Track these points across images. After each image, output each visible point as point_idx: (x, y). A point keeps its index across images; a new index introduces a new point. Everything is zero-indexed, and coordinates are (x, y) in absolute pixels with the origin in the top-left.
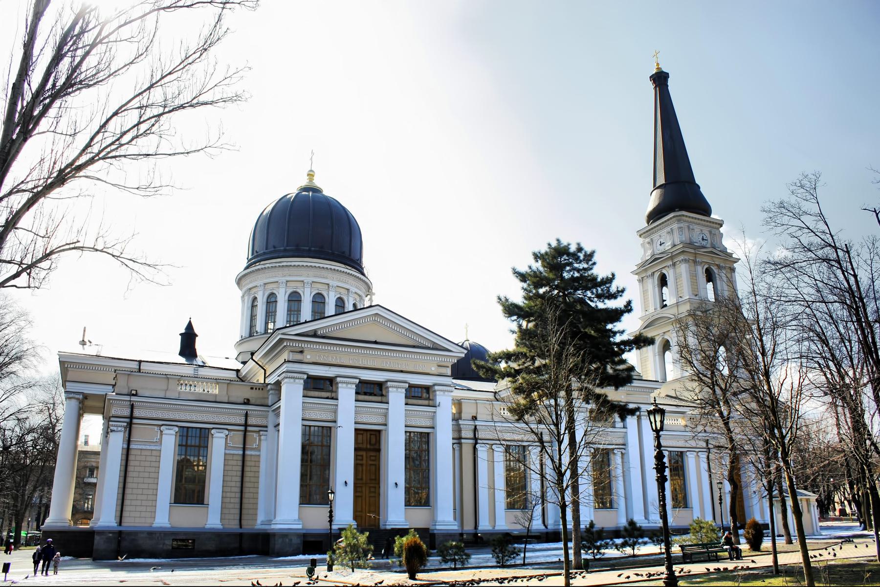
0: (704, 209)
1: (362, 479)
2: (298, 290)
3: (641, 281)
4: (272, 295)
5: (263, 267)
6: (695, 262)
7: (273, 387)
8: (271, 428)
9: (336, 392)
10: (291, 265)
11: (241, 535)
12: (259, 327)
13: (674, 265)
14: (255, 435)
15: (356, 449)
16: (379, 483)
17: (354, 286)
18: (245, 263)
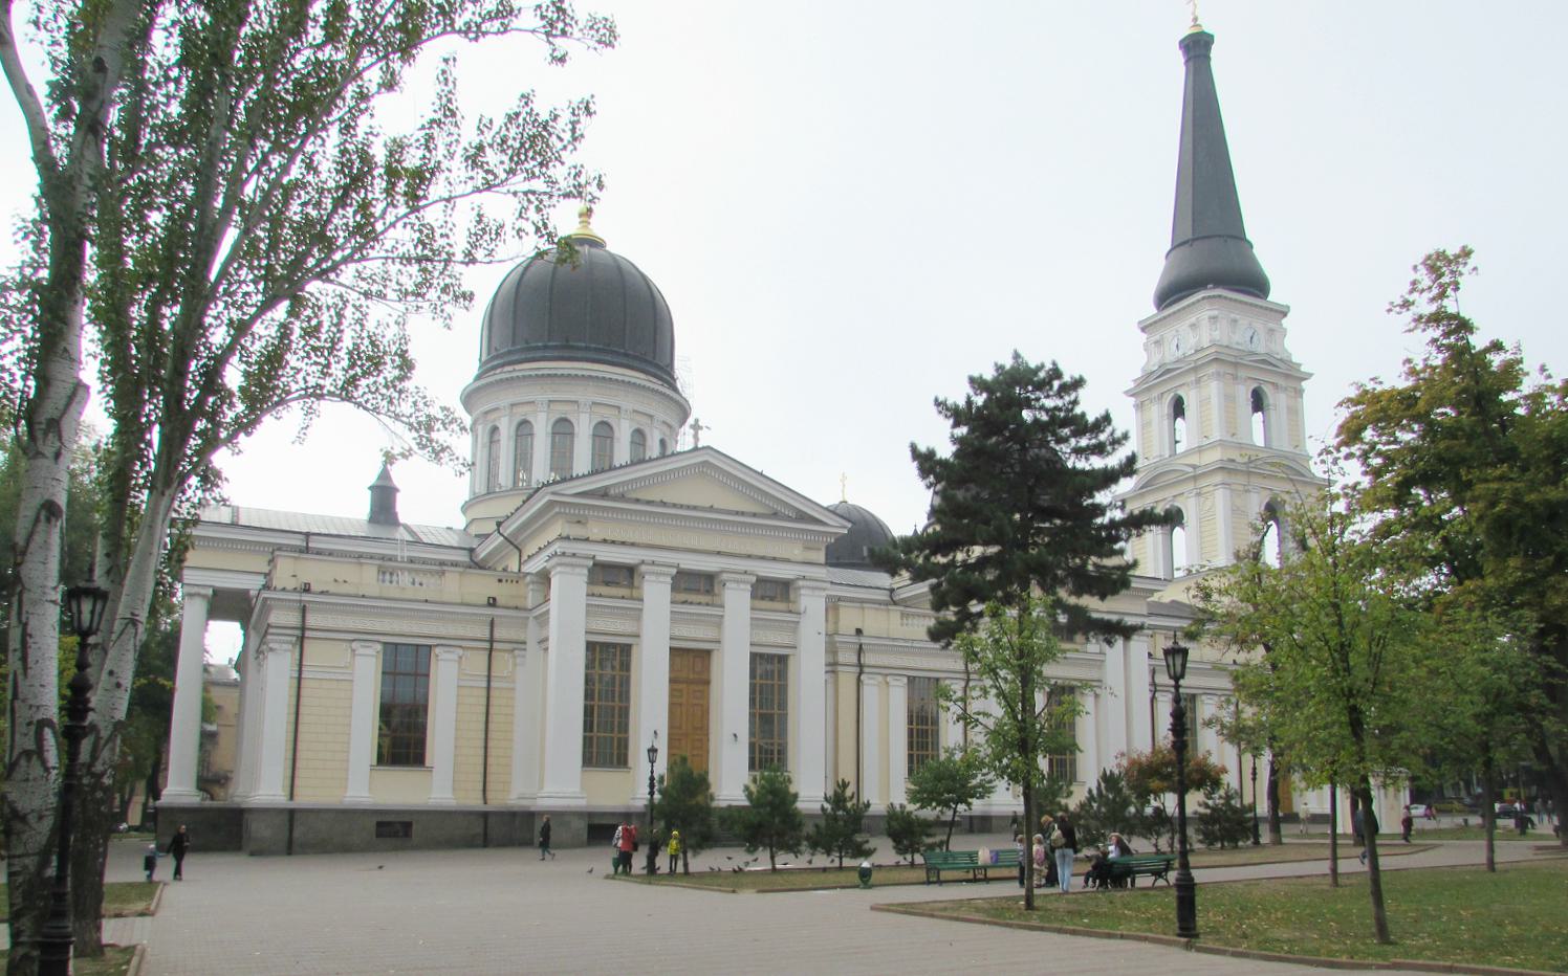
0: (1253, 284)
1: (680, 728)
2: (569, 417)
3: (1140, 407)
4: (524, 423)
5: (508, 376)
6: (1235, 377)
7: (535, 579)
8: (532, 645)
10: (556, 375)
11: (485, 815)
12: (504, 478)
13: (1198, 381)
14: (507, 655)
15: (672, 681)
16: (708, 735)
17: (661, 412)
18: (474, 369)
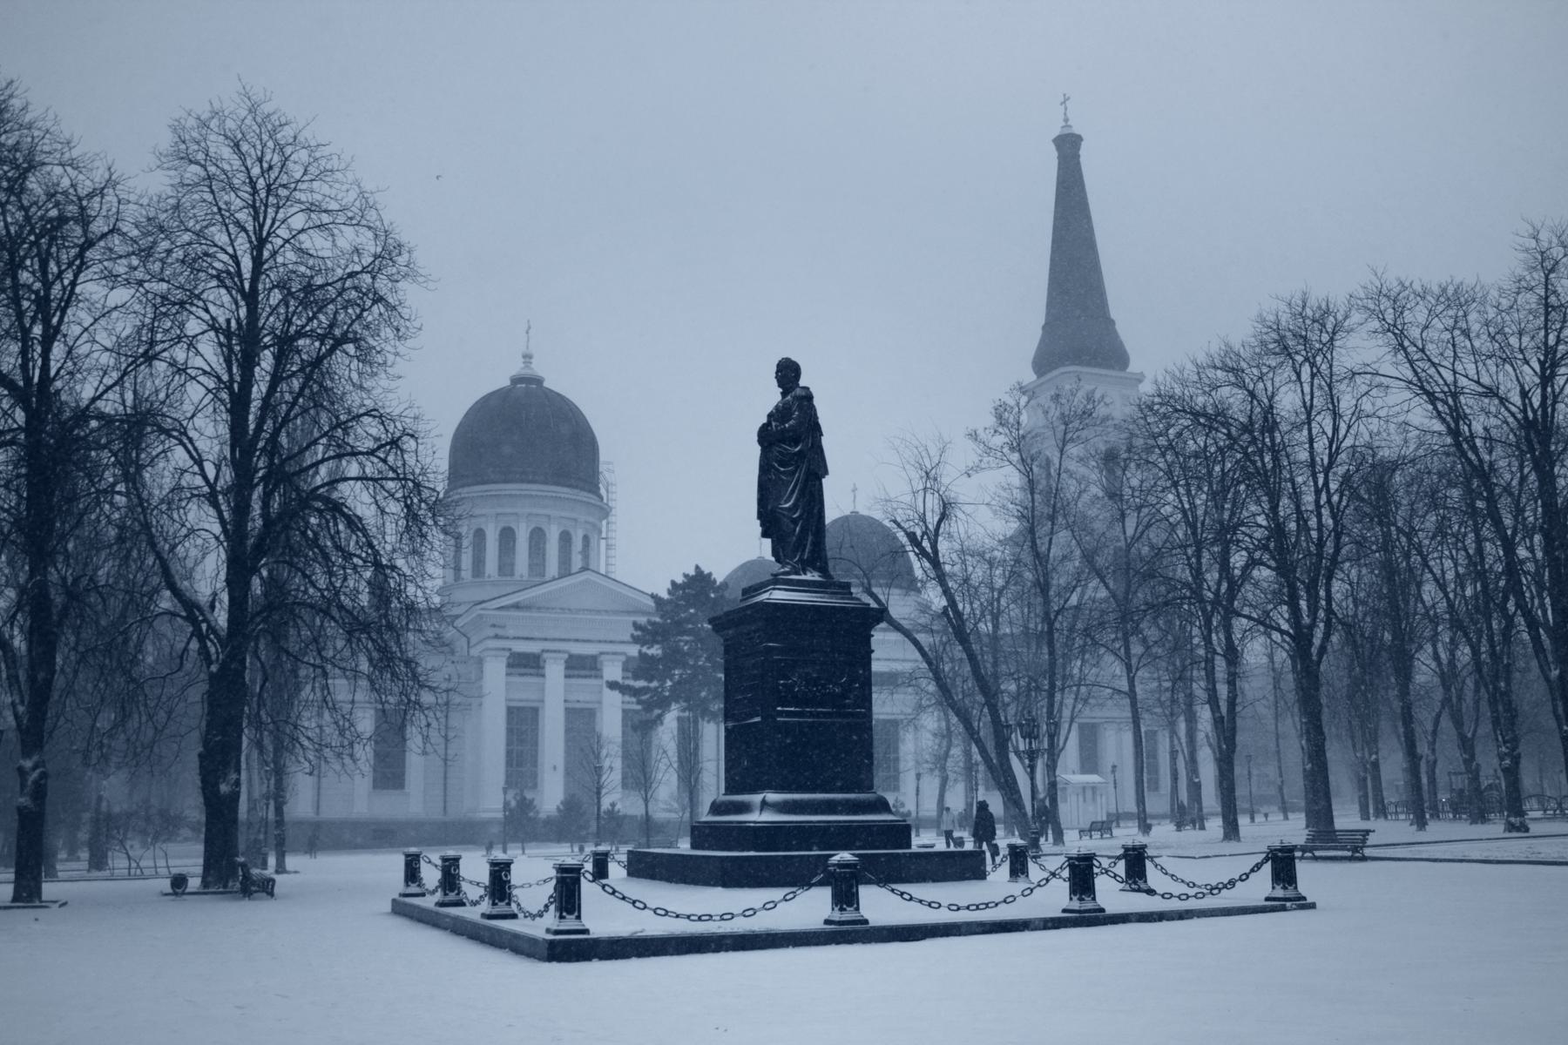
9: (543, 668)
